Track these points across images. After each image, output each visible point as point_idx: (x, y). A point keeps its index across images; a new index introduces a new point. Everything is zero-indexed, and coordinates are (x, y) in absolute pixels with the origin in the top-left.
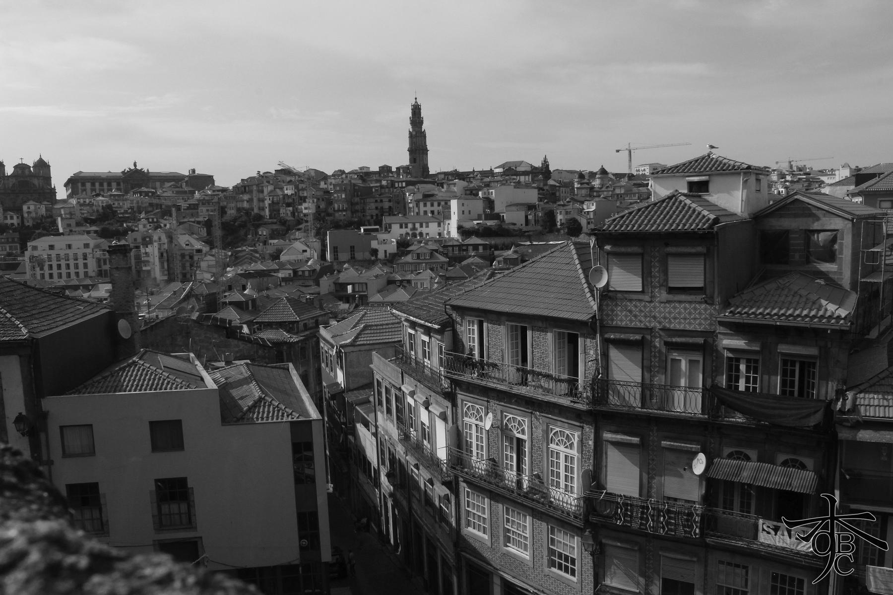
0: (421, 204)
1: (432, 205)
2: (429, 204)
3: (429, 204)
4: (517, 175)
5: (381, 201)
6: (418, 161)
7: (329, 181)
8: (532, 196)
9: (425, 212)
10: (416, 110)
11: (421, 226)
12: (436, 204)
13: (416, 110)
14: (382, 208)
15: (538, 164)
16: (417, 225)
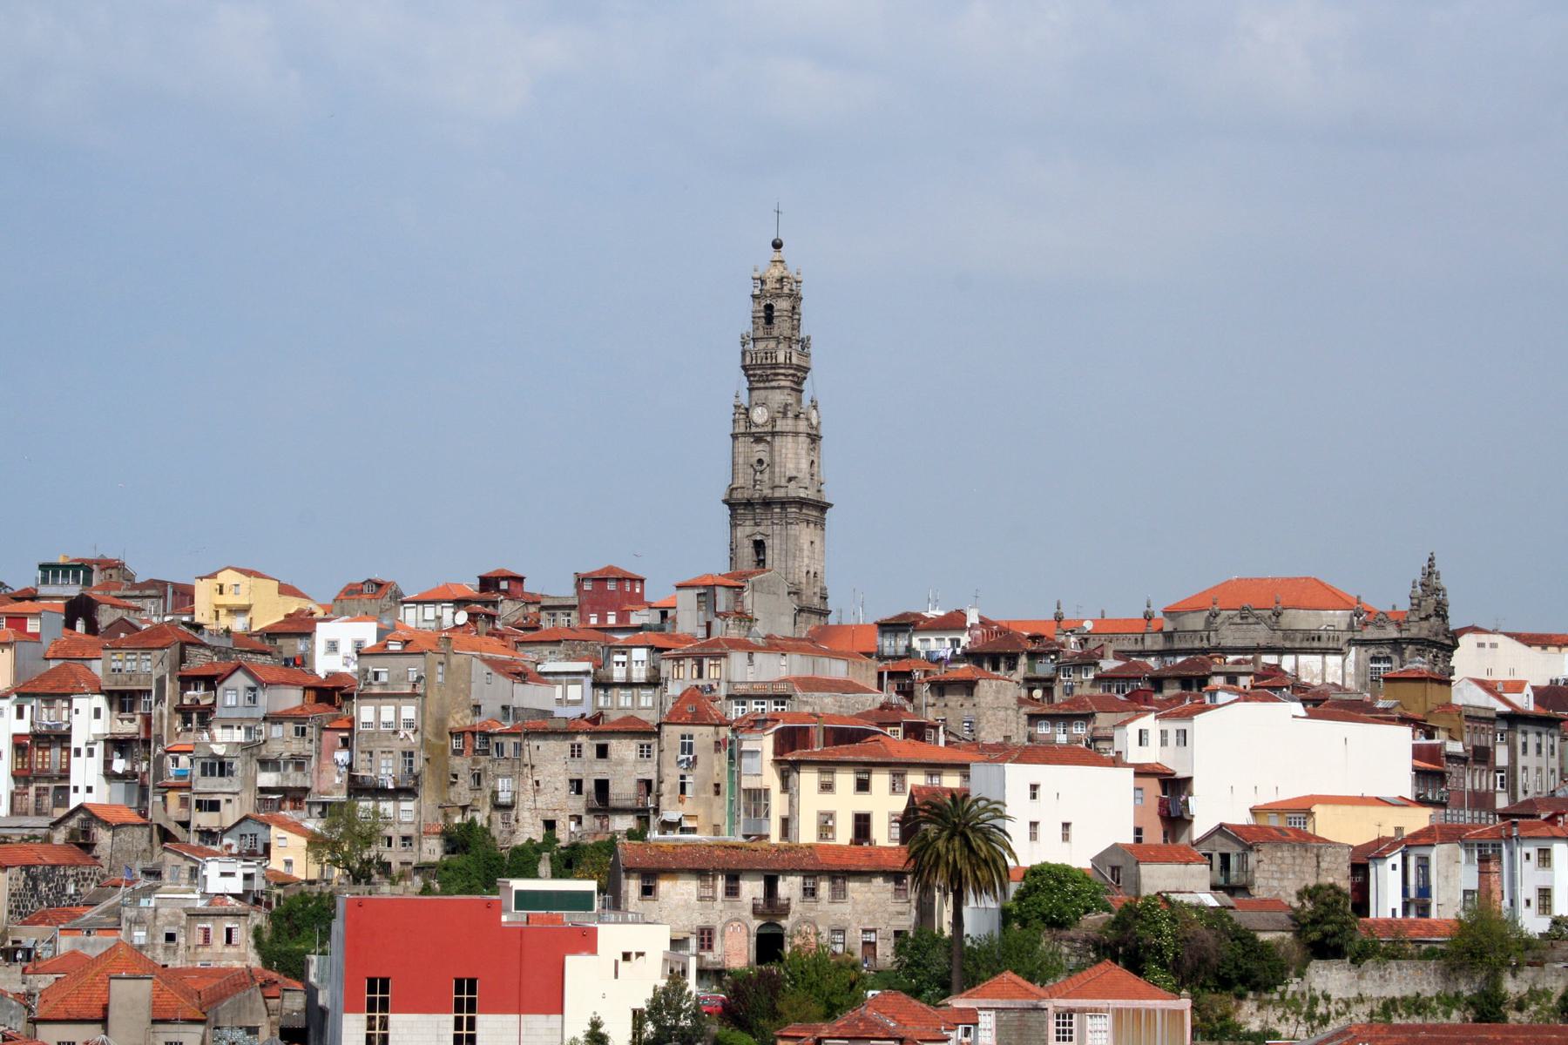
0: (808, 780)
1: (863, 786)
2: (845, 780)
3: (845, 780)
4: (1281, 651)
5: (602, 752)
6: (770, 555)
7: (324, 632)
8: (1379, 758)
9: (826, 823)
10: (775, 308)
11: (810, 892)
12: (880, 780)
13: (775, 308)
14: (602, 786)
15: (1391, 594)
16: (789, 887)
